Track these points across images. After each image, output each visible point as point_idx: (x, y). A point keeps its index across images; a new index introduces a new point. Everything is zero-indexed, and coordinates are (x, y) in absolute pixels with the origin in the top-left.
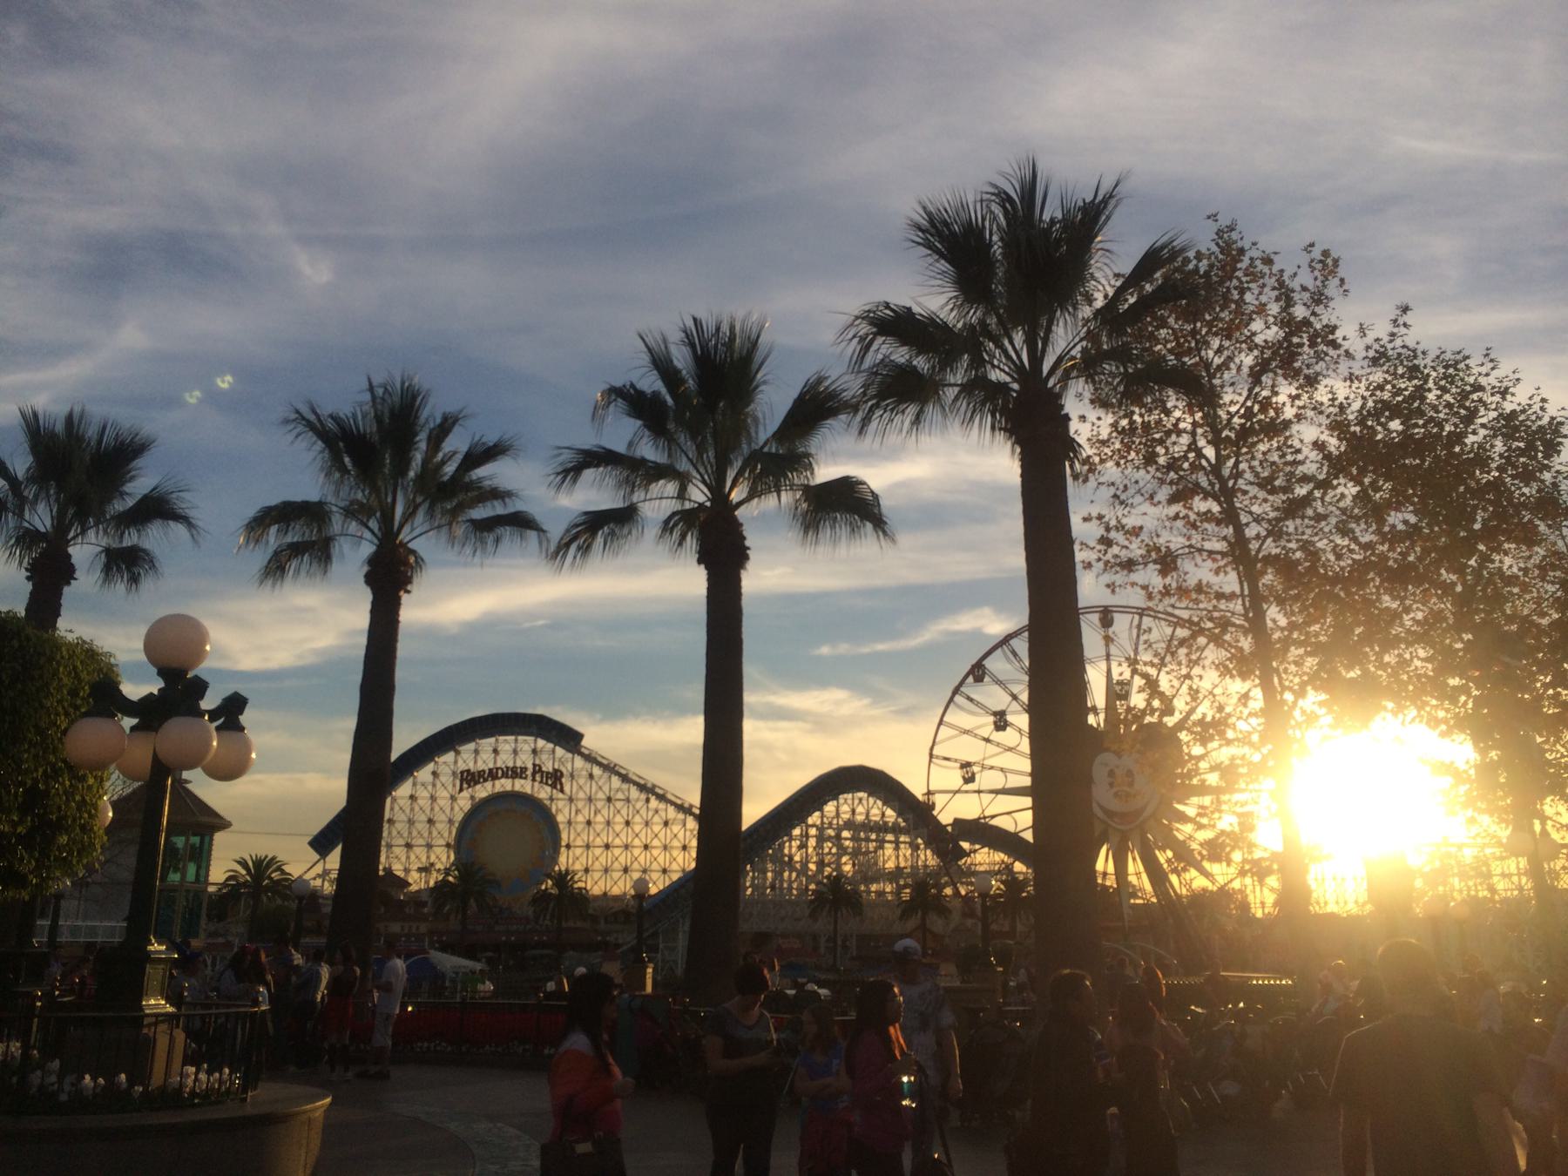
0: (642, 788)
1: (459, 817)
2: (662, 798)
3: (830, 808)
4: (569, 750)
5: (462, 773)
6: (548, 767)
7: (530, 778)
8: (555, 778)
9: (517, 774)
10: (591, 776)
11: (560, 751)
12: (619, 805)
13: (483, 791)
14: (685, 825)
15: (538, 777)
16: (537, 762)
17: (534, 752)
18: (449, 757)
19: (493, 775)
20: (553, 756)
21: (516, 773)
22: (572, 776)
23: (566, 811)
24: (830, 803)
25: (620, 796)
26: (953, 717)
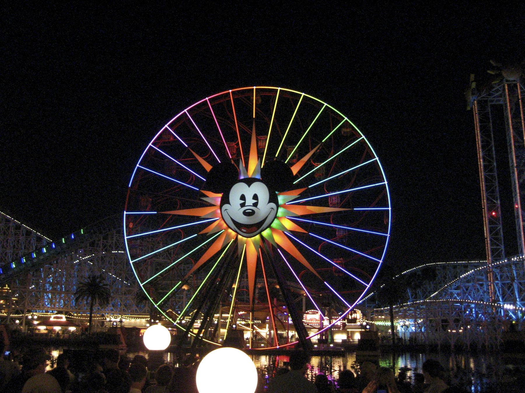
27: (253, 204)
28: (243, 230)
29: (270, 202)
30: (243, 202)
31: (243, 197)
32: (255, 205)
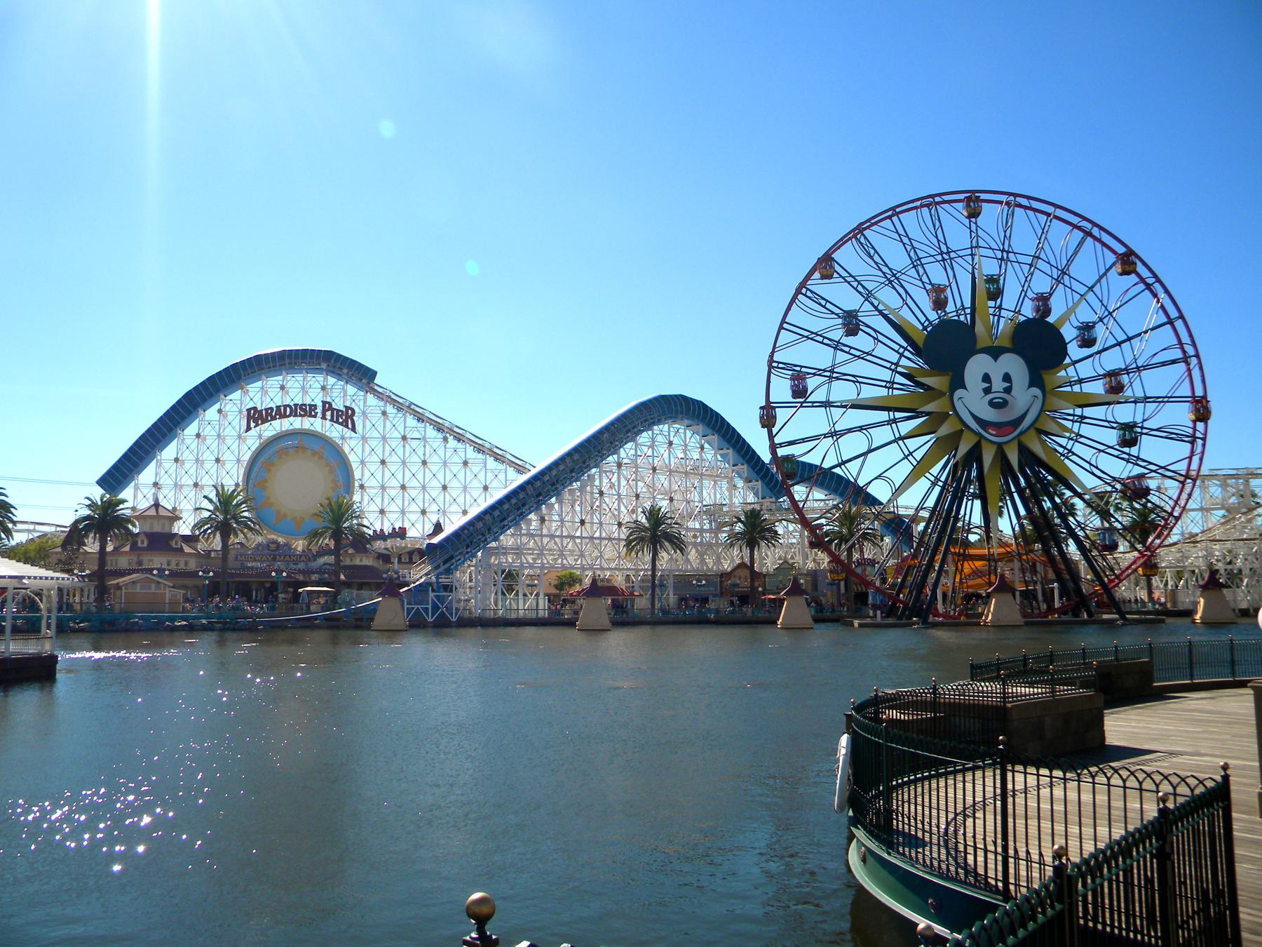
0: (439, 428)
1: (247, 457)
2: (459, 438)
3: (644, 438)
4: (360, 389)
5: (249, 410)
6: (339, 405)
7: (319, 415)
8: (345, 417)
9: (305, 410)
10: (384, 413)
11: (351, 390)
12: (415, 444)
13: (271, 429)
14: (485, 466)
15: (328, 414)
16: (328, 400)
17: (323, 388)
18: (237, 395)
19: (280, 412)
20: (343, 393)
21: (307, 410)
22: (364, 413)
23: (359, 450)
24: (644, 434)
25: (416, 435)
26: (795, 316)
27: (1004, 389)
28: (990, 431)
29: (1031, 385)
30: (988, 385)
31: (986, 378)
32: (1008, 390)
